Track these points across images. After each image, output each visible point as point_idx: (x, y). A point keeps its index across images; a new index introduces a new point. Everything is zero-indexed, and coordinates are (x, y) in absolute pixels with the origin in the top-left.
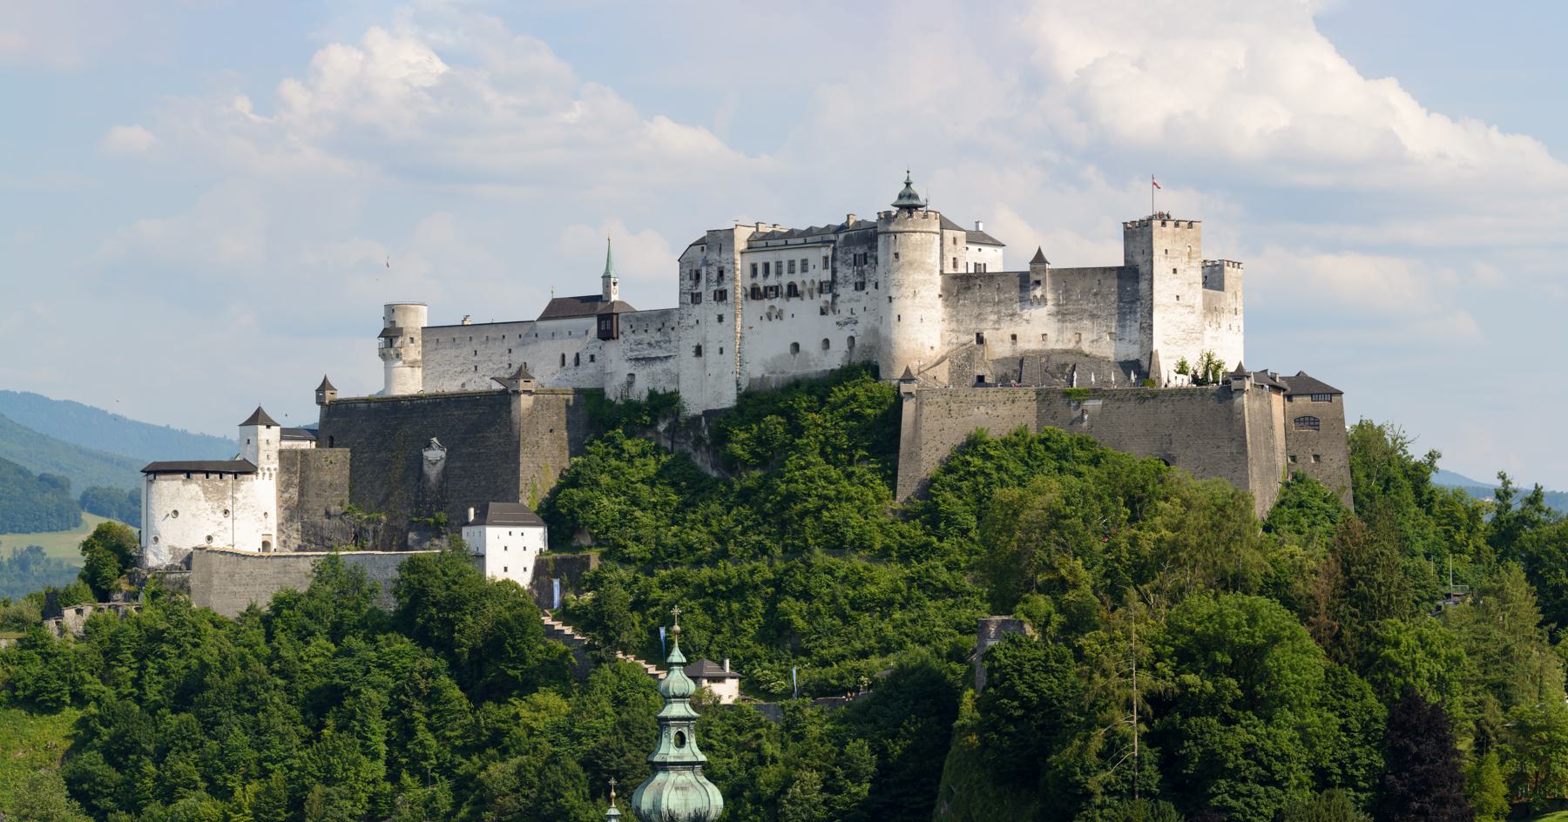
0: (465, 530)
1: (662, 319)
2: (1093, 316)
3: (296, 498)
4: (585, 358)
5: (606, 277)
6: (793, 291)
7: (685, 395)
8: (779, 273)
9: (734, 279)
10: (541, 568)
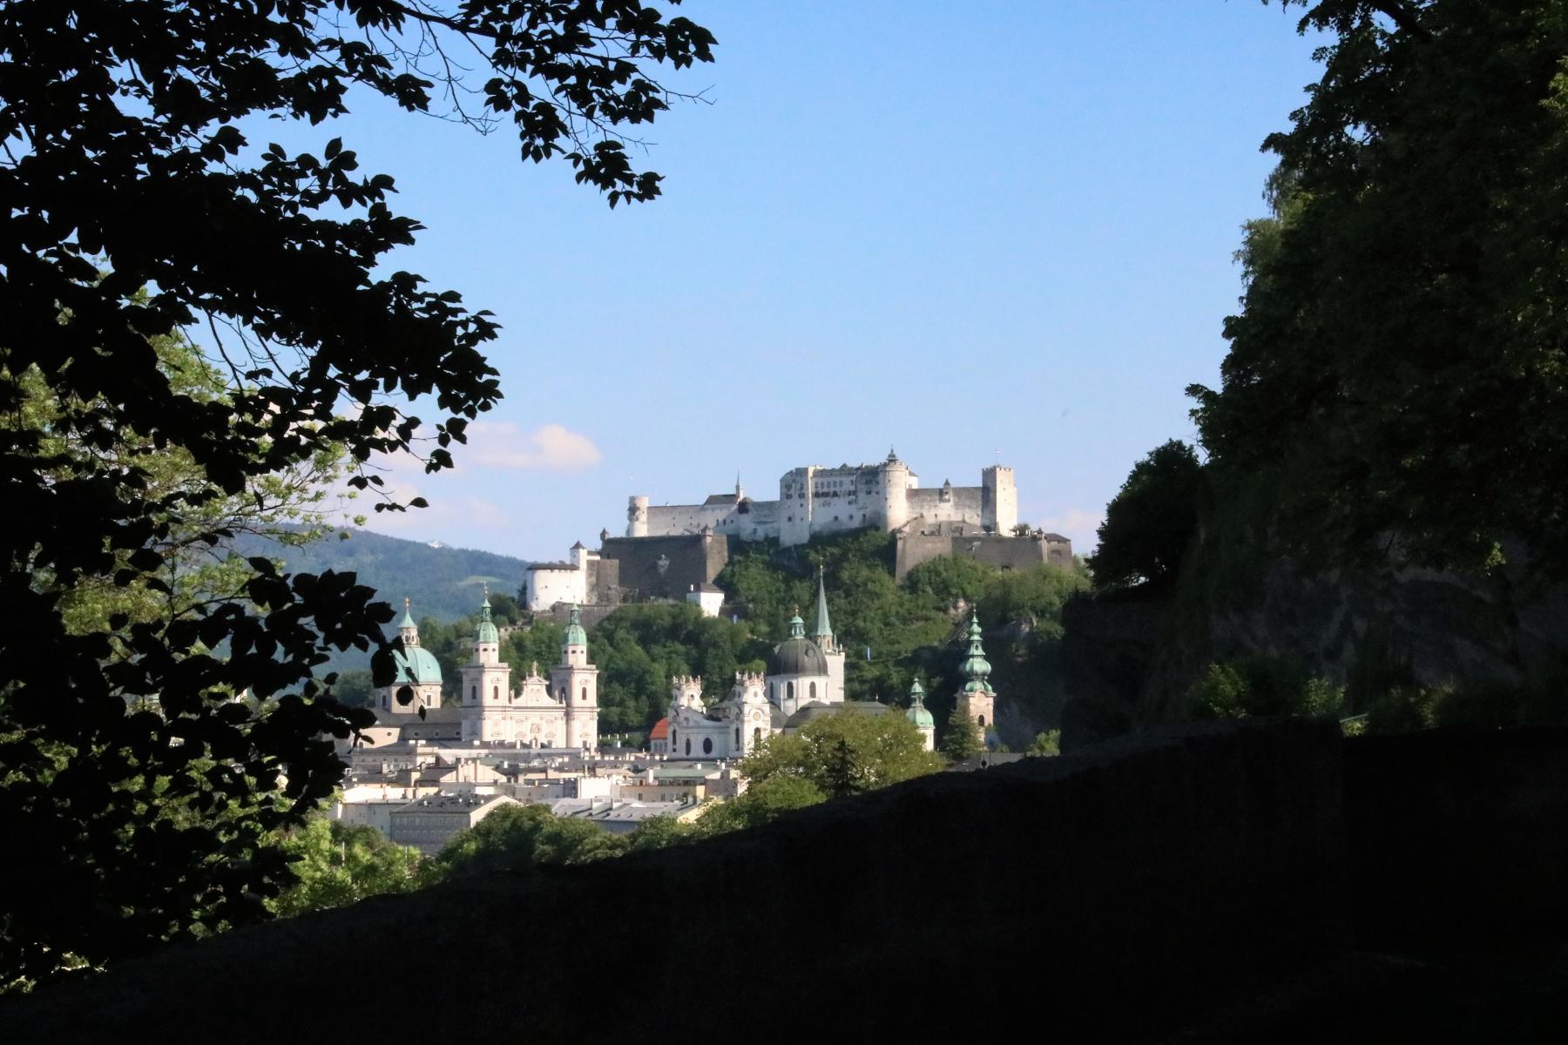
0: (688, 595)
1: (770, 505)
2: (969, 507)
3: (595, 581)
4: (728, 521)
5: (738, 488)
6: (835, 494)
7: (781, 539)
8: (829, 487)
9: (808, 488)
10: (722, 611)
